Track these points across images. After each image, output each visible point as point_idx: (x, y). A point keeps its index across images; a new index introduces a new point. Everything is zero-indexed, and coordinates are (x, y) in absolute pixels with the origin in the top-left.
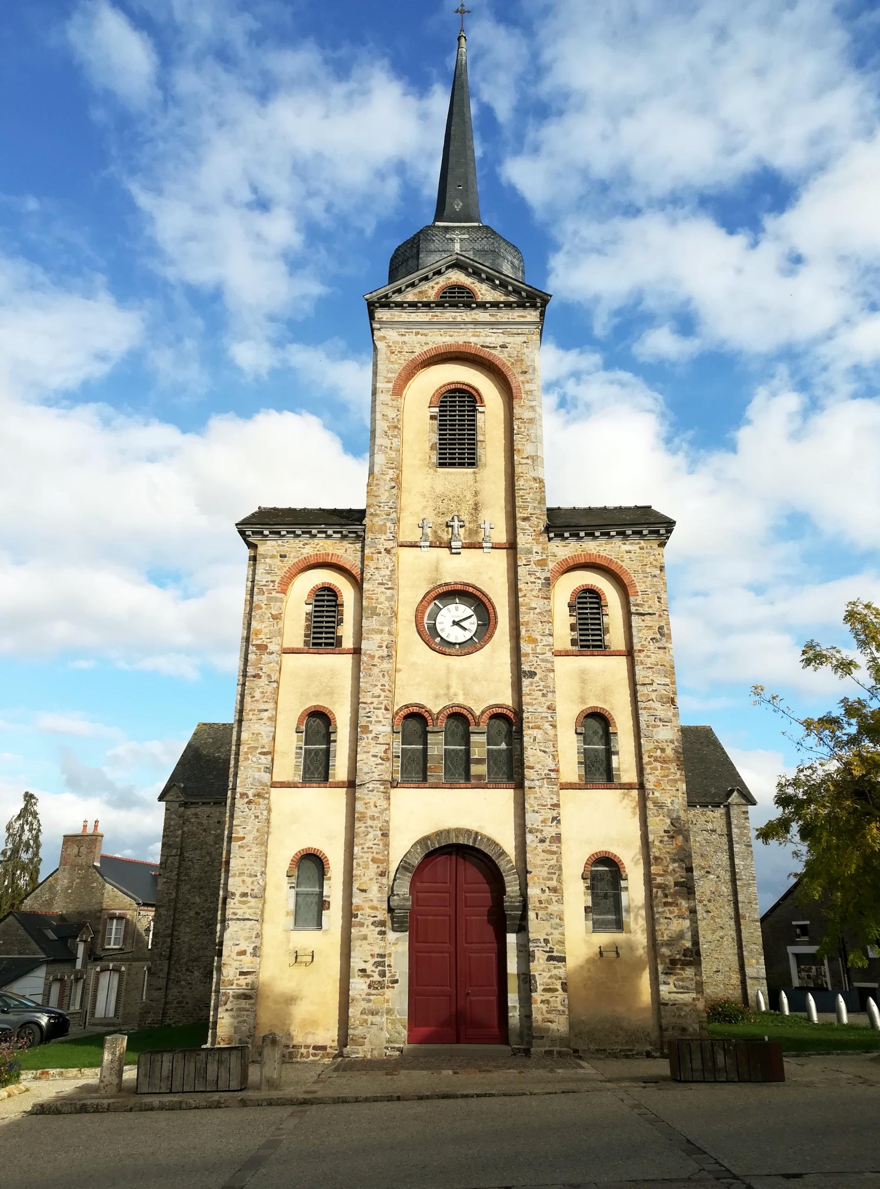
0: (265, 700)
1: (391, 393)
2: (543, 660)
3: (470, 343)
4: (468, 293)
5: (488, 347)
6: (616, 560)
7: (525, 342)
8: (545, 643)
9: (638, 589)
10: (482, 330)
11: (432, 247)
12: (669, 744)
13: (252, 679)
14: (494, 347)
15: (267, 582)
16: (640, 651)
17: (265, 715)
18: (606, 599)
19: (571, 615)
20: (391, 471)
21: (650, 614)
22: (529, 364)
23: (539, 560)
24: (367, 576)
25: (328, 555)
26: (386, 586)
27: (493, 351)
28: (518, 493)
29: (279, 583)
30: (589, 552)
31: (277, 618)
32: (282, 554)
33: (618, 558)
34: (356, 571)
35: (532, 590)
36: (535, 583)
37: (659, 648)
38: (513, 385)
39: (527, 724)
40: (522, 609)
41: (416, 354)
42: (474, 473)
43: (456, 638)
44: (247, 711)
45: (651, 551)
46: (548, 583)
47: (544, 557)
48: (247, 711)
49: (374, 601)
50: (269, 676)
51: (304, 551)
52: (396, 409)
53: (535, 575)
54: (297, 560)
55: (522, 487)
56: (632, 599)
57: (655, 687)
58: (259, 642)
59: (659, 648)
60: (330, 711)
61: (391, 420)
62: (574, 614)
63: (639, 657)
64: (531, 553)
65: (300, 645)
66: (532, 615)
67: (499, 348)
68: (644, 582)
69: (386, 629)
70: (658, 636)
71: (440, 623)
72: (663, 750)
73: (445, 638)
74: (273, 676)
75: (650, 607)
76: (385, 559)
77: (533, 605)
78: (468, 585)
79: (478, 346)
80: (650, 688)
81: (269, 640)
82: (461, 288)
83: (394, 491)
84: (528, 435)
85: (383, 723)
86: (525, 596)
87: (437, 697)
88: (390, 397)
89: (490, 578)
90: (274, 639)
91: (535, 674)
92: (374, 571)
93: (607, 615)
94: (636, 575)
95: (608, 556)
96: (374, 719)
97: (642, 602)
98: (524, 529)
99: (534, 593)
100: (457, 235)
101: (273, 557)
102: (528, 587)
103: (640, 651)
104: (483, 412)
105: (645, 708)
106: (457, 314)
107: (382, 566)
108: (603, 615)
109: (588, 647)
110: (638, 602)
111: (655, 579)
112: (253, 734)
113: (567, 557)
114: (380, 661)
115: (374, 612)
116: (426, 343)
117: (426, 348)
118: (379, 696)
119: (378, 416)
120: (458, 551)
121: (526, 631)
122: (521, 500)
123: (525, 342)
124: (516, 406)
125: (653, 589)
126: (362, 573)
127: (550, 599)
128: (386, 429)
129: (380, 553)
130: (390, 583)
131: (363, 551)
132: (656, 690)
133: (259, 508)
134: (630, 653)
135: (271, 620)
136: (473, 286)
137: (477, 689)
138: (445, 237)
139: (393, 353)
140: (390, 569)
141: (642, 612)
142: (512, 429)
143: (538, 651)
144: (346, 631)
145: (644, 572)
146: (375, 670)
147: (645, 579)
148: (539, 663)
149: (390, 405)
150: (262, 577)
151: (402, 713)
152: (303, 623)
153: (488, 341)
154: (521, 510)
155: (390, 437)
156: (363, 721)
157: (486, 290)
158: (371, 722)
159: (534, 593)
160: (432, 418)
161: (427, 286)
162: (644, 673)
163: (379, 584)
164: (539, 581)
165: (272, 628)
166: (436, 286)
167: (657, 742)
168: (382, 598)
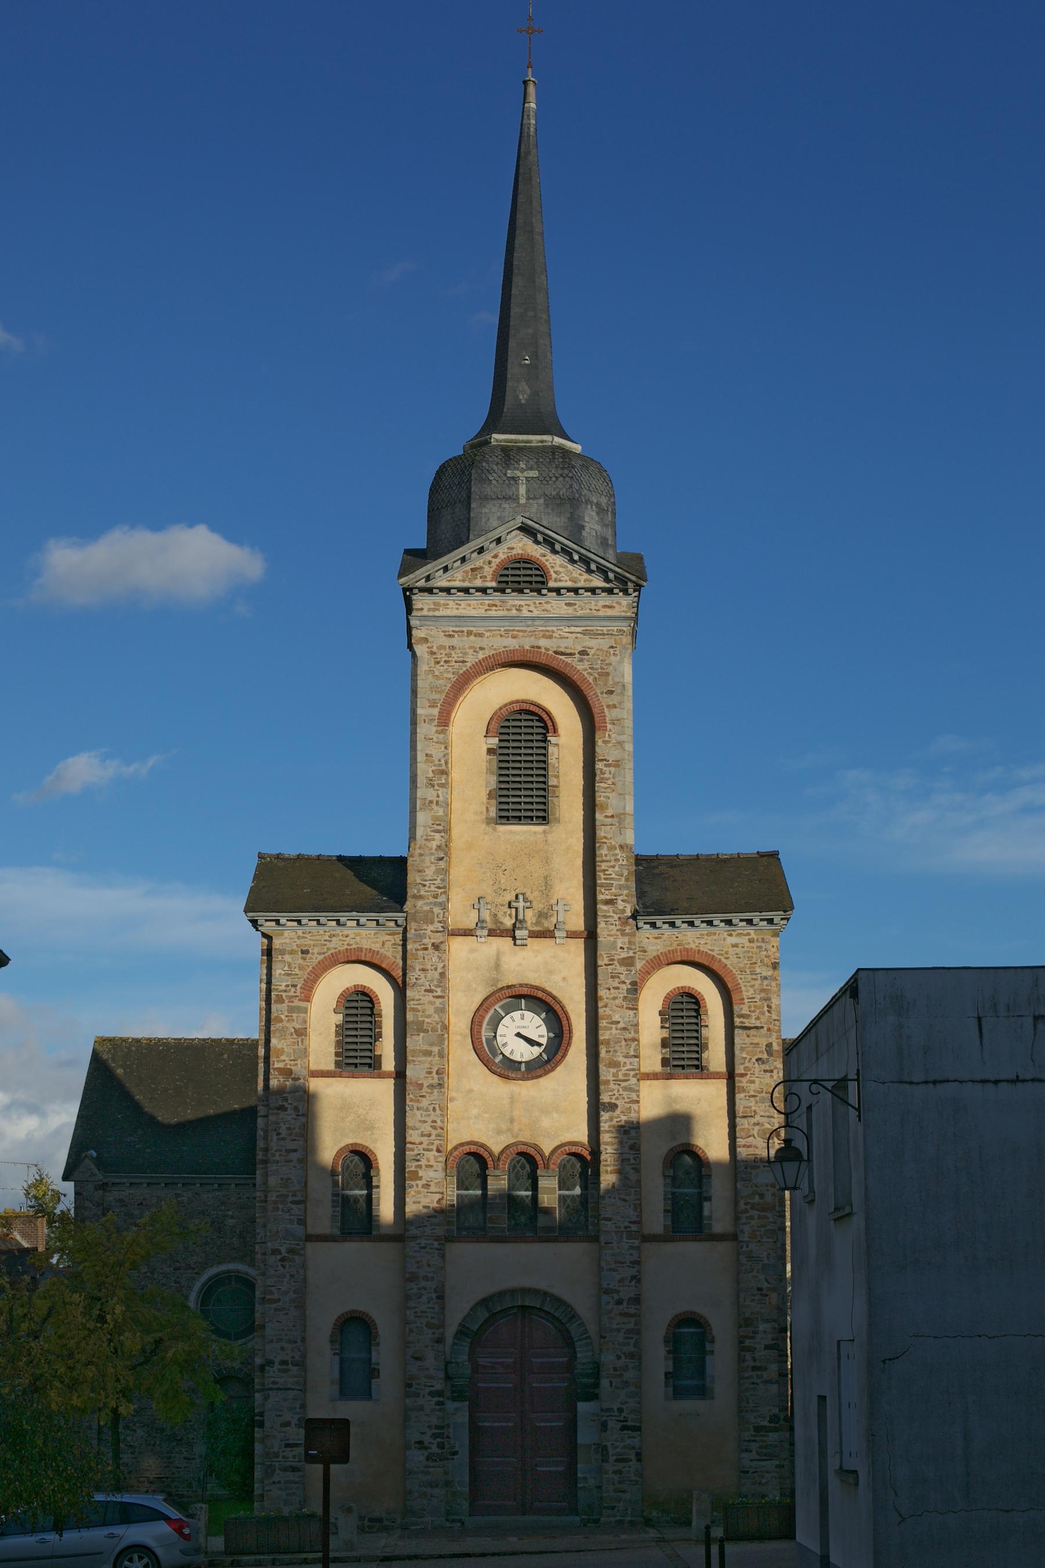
0: (293, 1137)
1: (436, 722)
2: (625, 1089)
3: (539, 648)
4: (536, 569)
5: (563, 654)
6: (719, 957)
7: (612, 647)
8: (629, 1067)
9: (745, 994)
10: (555, 629)
11: (488, 490)
12: (769, 1188)
13: (275, 1111)
14: (571, 654)
15: (287, 986)
16: (742, 1075)
17: (294, 1156)
18: (706, 1006)
19: (662, 1027)
20: (437, 836)
21: (756, 1028)
22: (617, 680)
23: (624, 958)
24: (411, 977)
25: (362, 951)
26: (435, 994)
27: (569, 660)
28: (600, 866)
29: (301, 988)
30: (687, 947)
31: (301, 1035)
32: (304, 949)
33: (722, 955)
34: (398, 973)
35: (614, 998)
36: (618, 988)
37: (765, 1071)
38: (595, 710)
39: (605, 1168)
40: (603, 1023)
41: (469, 665)
42: (544, 832)
43: (522, 1056)
44: (273, 1151)
45: (763, 945)
46: (635, 989)
47: (631, 954)
48: (273, 1151)
49: (420, 1014)
50: (296, 1109)
51: (332, 945)
52: (443, 747)
53: (619, 977)
54: (320, 957)
55: (604, 858)
56: (736, 1008)
57: (757, 1118)
58: (281, 1065)
59: (765, 1071)
60: (370, 1150)
61: (437, 762)
62: (667, 1025)
63: (741, 1082)
64: (615, 948)
65: (331, 1067)
66: (614, 1031)
67: (577, 656)
68: (752, 986)
69: (435, 1049)
70: (765, 1056)
71: (501, 1036)
72: (762, 1196)
73: (508, 1055)
74: (300, 1108)
75: (758, 1018)
76: (433, 956)
77: (616, 1018)
78: (537, 988)
79: (551, 653)
80: (753, 1121)
81: (292, 1062)
82: (525, 563)
83: (442, 864)
84: (613, 784)
85: (435, 1168)
86: (606, 1006)
87: (499, 1132)
88: (434, 729)
89: (564, 979)
90: (299, 1062)
91: (615, 1106)
92: (419, 973)
93: (707, 1026)
94: (742, 977)
95: (710, 952)
96: (423, 1162)
97: (748, 1013)
98: (605, 916)
99: (618, 1002)
100: (522, 471)
101: (292, 952)
102: (610, 994)
103: (742, 1075)
104: (557, 745)
105: (744, 1146)
106: (522, 603)
107: (429, 967)
108: (701, 1026)
109: (683, 1067)
110: (743, 1012)
111: (766, 982)
112: (282, 1179)
113: (659, 953)
114: (429, 1090)
115: (421, 1029)
116: (482, 649)
117: (481, 656)
118: (429, 1135)
119: (420, 757)
120: (524, 942)
121: (607, 1052)
122: (603, 876)
123: (612, 647)
124: (599, 742)
125: (763, 995)
126: (404, 975)
127: (636, 1009)
128: (431, 775)
129: (426, 949)
130: (439, 990)
131: (404, 945)
132: (758, 1124)
133: (261, 856)
134: (731, 1076)
135: (295, 1036)
136: (543, 559)
137: (546, 1123)
138: (505, 474)
139: (438, 663)
140: (440, 970)
141: (747, 1025)
142: (594, 820)
143: (621, 1077)
144: (386, 1048)
145: (753, 973)
146: (425, 1103)
147: (753, 983)
148: (621, 1092)
149: (435, 740)
150: (280, 982)
151: (456, 1153)
152: (332, 1037)
153: (563, 644)
154: (603, 891)
155: (436, 787)
156: (411, 1166)
157: (561, 566)
158: (420, 1167)
159: (618, 1002)
160: (490, 751)
161: (482, 561)
162: (744, 1103)
163: (426, 991)
164: (624, 987)
165: (296, 1047)
166: (493, 560)
167: (756, 1186)
168: (430, 1010)
